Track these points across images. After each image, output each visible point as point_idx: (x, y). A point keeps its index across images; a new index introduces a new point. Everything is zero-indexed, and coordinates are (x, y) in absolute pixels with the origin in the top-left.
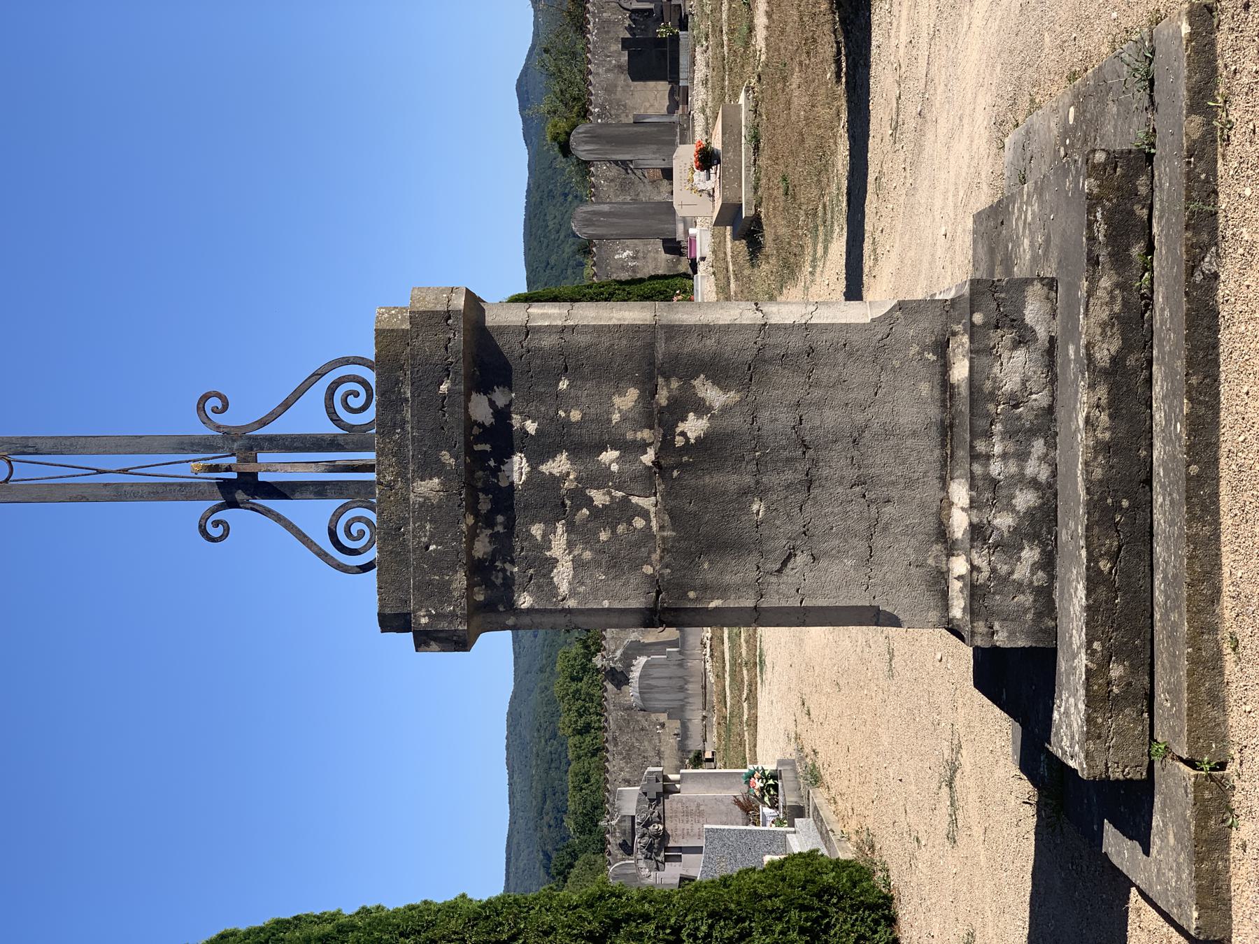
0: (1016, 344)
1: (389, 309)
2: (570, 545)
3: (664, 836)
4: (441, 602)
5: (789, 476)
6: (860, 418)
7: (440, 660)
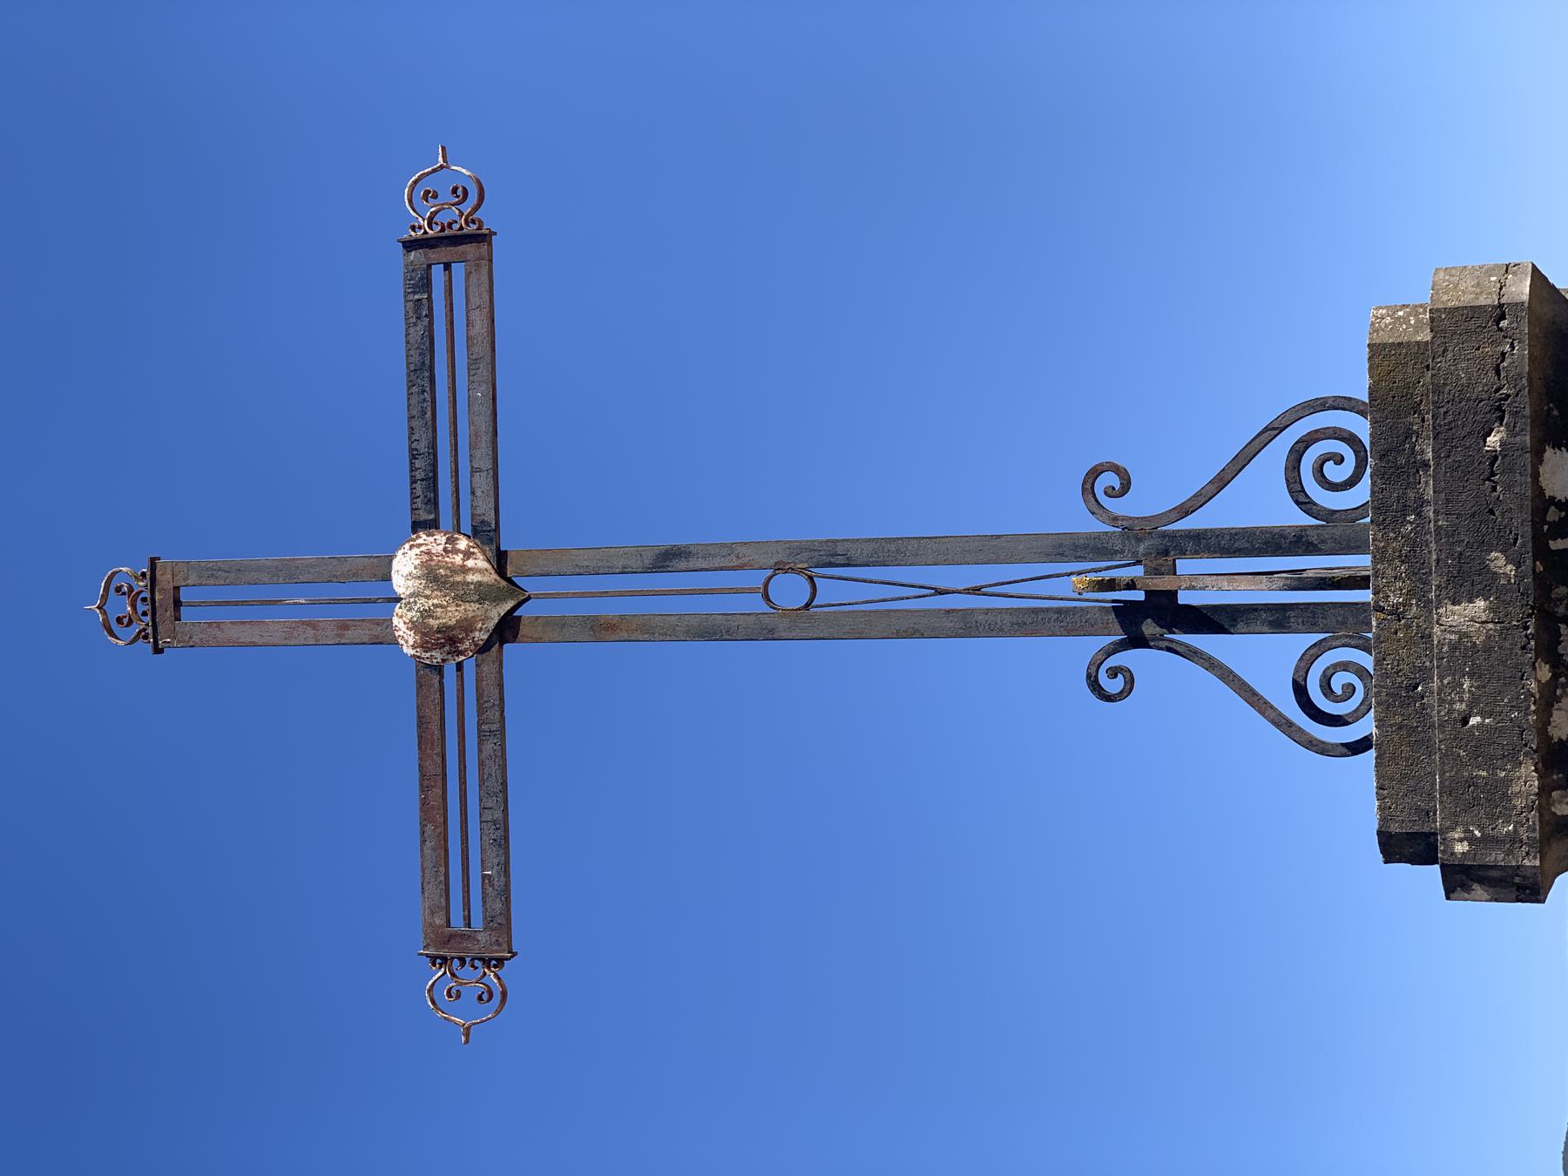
1: (1393, 310)
4: (1493, 818)
7: (1487, 915)
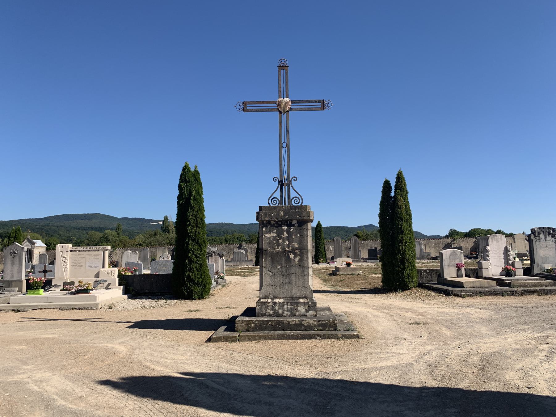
0: (306, 310)
2: (273, 236)
5: (284, 272)
6: (293, 284)
7: (255, 215)
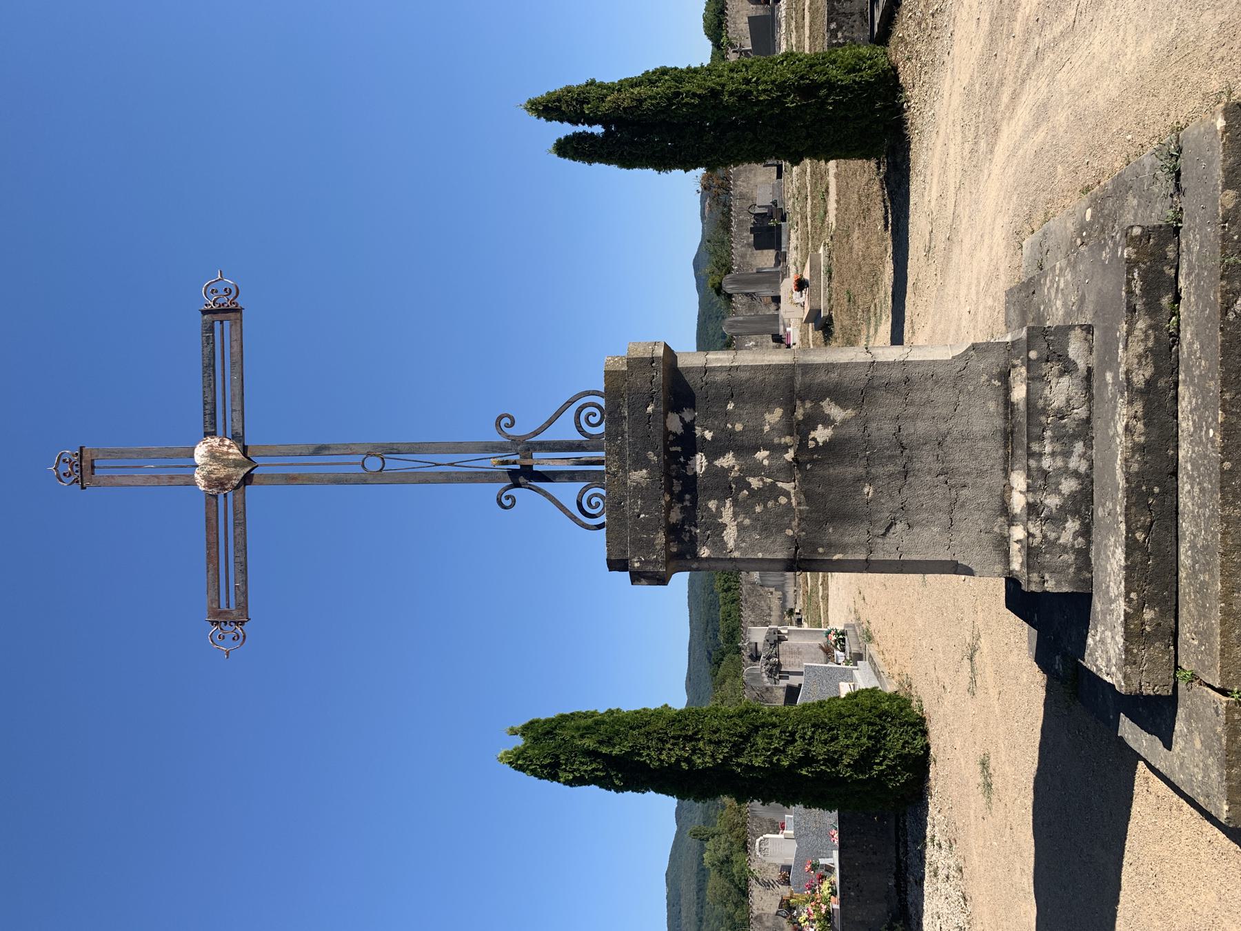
0: (1062, 373)
1: (613, 358)
2: (735, 515)
3: (779, 665)
4: (649, 553)
5: (891, 468)
6: (943, 427)
7: (647, 591)
